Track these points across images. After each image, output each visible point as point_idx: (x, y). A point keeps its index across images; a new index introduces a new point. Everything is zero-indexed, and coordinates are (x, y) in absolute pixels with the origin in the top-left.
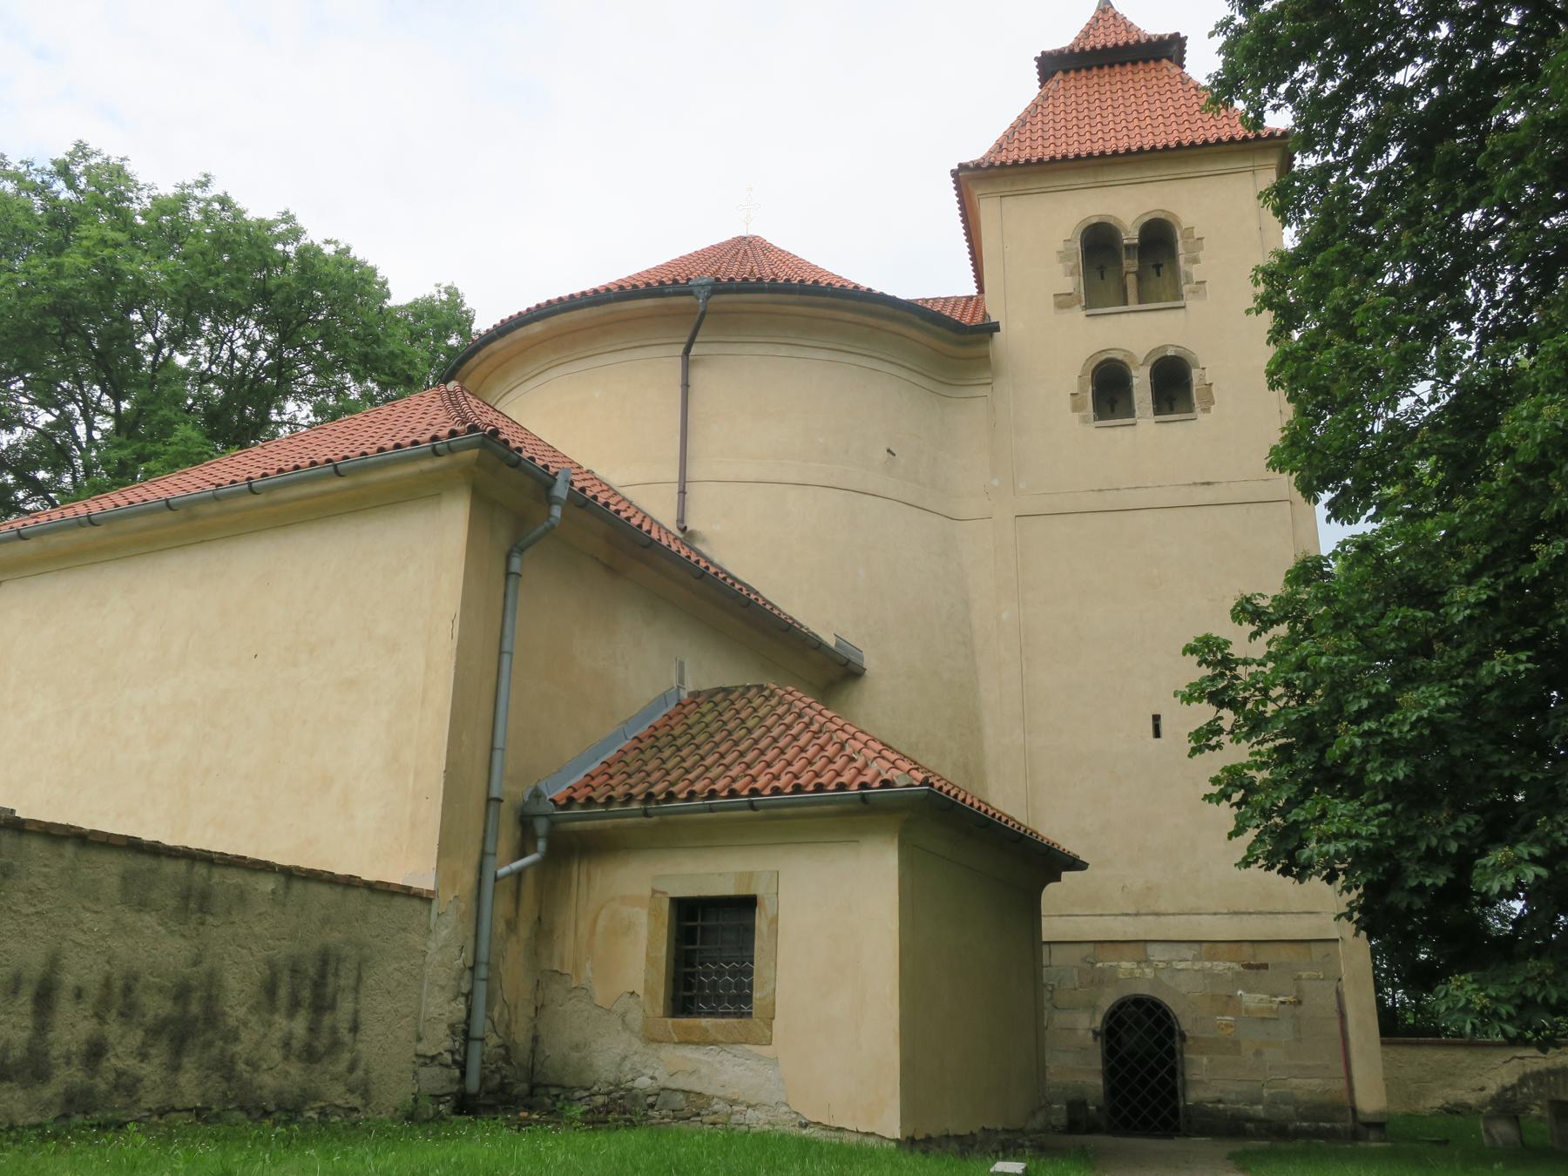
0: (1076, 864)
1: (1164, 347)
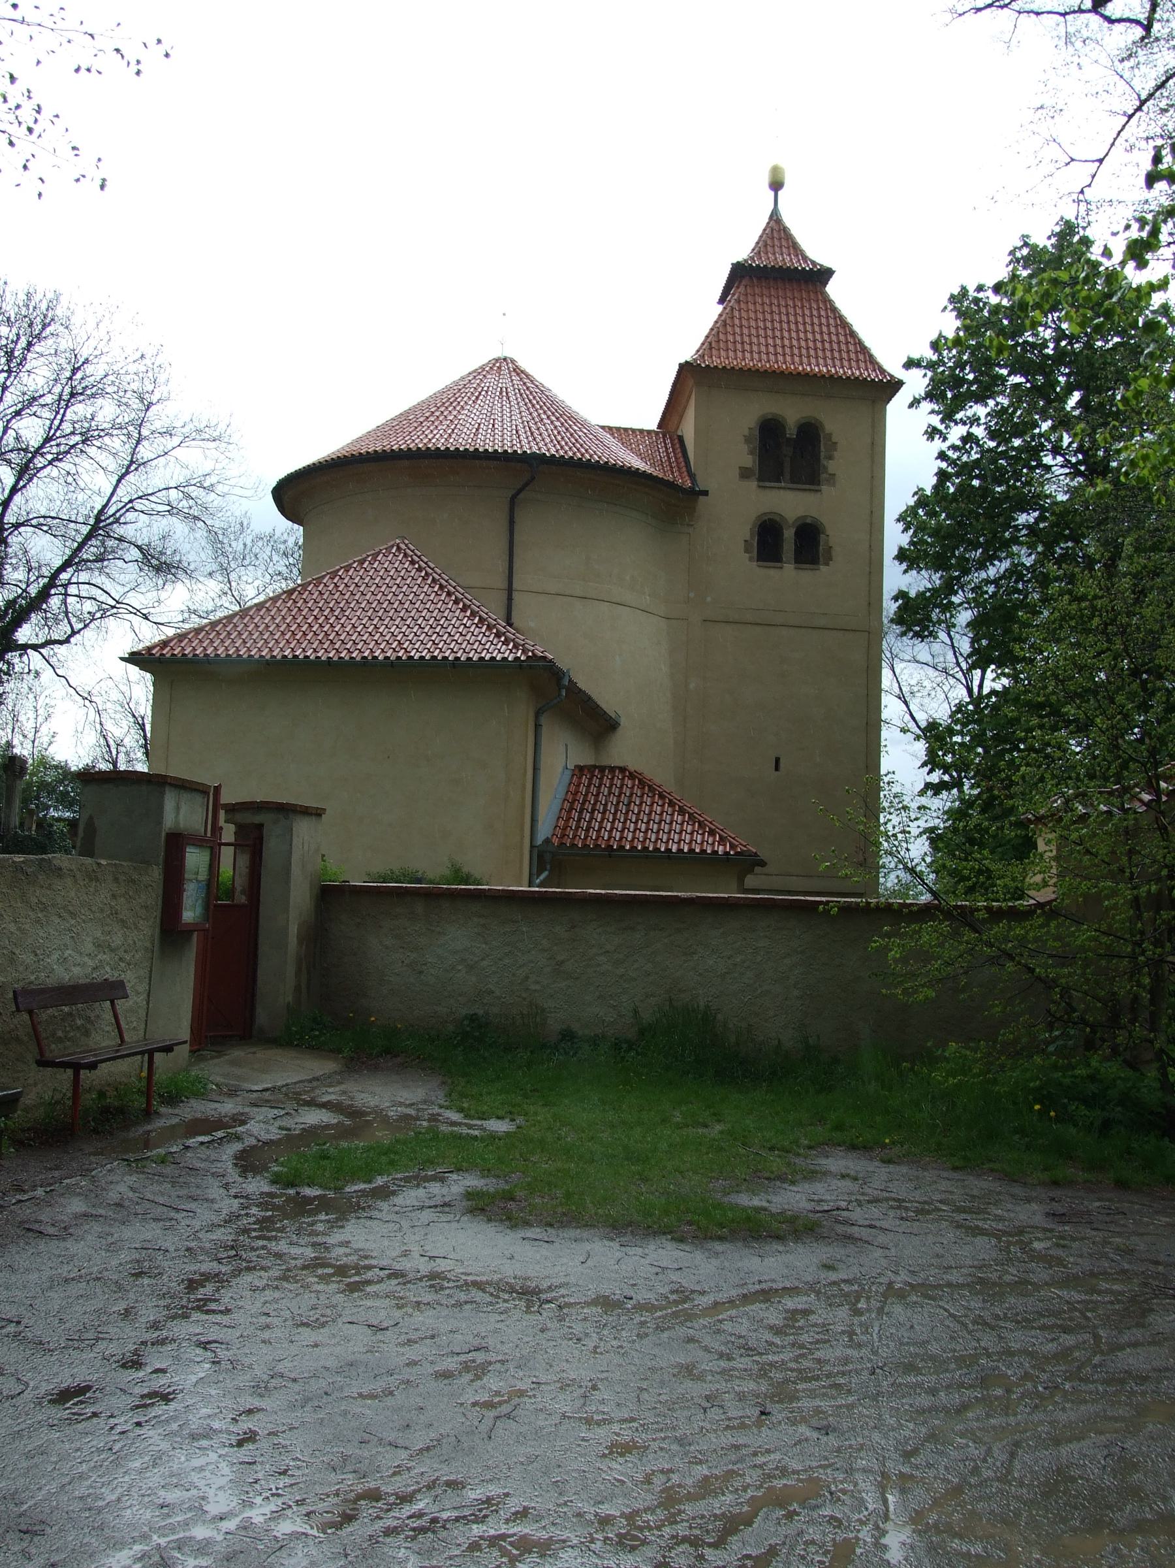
0: (762, 864)
1: (806, 516)
